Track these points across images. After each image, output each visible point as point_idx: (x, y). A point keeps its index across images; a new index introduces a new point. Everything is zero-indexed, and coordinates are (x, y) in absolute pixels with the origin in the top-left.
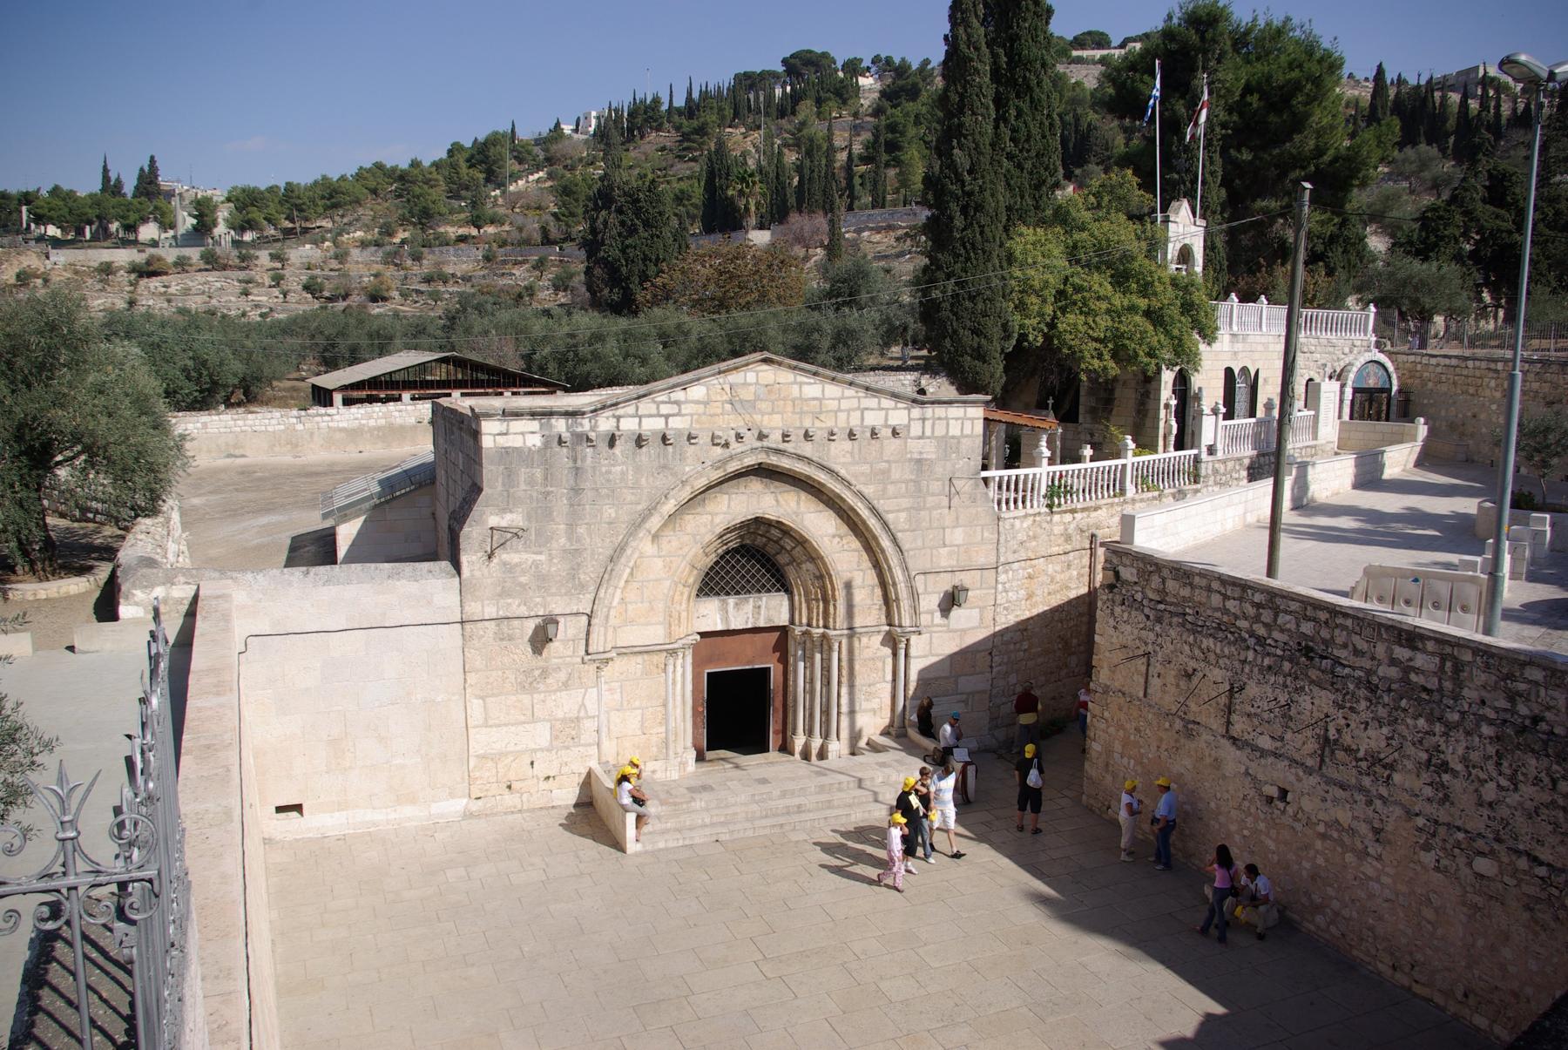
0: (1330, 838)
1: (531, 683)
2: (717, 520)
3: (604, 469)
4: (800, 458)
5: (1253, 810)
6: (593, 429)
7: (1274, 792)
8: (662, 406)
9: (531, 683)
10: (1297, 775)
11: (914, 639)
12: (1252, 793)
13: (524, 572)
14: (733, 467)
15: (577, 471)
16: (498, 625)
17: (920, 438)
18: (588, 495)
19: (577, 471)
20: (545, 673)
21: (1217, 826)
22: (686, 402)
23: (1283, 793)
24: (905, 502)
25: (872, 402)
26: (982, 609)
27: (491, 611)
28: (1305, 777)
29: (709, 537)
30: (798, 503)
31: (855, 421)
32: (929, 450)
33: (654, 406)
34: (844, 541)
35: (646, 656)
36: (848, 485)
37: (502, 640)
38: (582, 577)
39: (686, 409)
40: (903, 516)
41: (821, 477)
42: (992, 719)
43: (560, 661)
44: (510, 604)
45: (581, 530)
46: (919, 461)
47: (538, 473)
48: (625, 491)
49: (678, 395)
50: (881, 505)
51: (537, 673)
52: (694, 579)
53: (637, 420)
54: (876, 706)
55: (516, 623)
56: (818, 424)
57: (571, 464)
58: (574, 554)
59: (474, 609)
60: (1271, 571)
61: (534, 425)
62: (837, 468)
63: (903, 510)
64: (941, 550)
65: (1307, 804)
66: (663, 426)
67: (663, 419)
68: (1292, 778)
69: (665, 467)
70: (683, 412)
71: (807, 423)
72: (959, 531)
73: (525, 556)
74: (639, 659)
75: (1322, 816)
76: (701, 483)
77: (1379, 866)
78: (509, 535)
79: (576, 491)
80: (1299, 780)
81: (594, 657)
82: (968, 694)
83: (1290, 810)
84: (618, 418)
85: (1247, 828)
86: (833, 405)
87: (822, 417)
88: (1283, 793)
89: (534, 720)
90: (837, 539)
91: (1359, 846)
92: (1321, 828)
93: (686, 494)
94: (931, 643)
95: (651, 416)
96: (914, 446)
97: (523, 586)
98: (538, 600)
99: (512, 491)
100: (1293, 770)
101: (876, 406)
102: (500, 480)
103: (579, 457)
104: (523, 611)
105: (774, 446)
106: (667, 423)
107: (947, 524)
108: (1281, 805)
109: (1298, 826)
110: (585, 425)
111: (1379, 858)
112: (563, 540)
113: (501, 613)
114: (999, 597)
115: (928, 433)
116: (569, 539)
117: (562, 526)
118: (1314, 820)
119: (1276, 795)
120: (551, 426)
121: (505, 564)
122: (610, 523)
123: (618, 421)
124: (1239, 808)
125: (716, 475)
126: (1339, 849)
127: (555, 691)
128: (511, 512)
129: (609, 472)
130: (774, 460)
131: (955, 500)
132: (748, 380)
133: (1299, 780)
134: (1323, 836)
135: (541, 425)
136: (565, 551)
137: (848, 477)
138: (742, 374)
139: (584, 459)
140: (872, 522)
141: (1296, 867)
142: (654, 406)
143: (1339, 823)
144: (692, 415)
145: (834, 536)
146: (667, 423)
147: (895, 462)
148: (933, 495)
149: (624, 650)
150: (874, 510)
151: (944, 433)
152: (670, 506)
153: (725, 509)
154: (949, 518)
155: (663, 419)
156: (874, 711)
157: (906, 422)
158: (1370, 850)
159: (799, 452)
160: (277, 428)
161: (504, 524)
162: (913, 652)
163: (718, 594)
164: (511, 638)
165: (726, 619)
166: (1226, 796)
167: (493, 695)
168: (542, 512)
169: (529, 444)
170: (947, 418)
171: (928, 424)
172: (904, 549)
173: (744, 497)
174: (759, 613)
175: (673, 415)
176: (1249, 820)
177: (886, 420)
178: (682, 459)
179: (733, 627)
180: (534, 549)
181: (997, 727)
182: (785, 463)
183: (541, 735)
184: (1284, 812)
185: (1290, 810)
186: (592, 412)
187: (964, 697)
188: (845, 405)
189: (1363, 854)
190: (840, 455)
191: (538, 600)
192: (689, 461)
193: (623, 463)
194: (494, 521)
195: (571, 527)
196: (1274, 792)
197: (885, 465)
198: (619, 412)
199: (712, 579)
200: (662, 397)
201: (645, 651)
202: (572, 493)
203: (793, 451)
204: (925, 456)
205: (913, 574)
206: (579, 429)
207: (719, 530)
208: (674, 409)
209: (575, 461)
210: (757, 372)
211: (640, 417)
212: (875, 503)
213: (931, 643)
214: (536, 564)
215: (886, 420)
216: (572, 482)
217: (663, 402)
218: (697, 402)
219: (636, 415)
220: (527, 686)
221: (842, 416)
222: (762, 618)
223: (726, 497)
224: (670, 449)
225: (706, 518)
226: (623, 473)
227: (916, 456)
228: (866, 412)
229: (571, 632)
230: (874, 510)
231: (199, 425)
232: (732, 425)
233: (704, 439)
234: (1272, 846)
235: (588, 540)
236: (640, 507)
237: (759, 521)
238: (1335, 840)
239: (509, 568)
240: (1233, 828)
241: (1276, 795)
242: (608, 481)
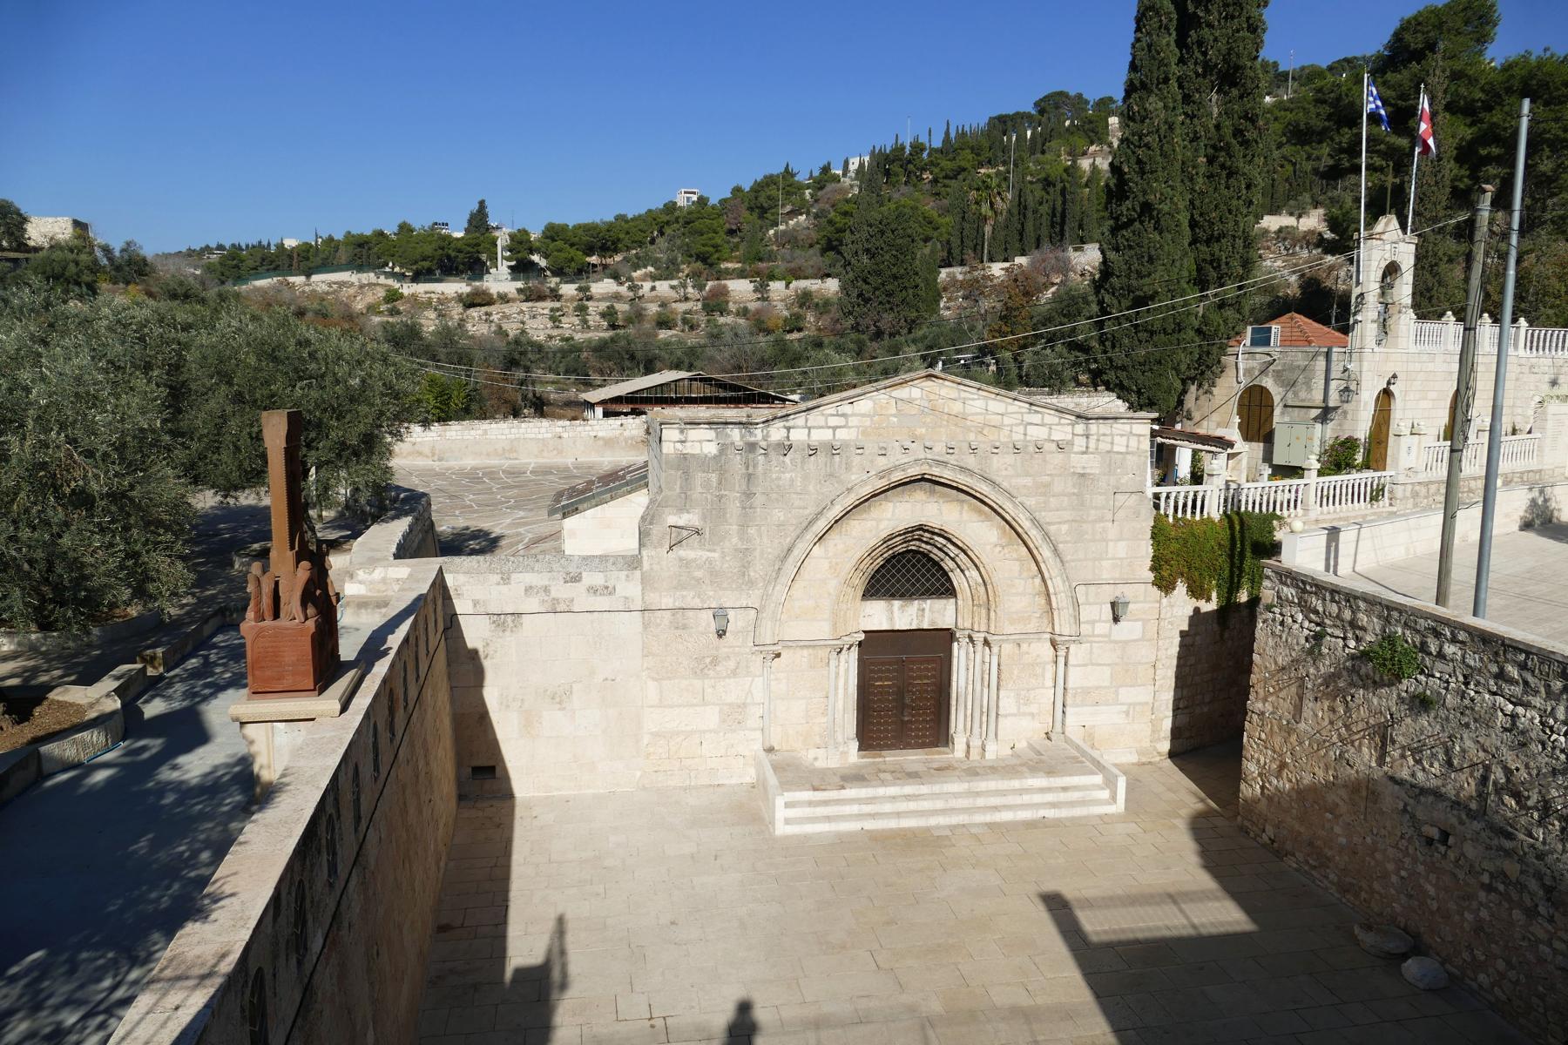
0: (1496, 890)
1: (702, 670)
2: (882, 527)
3: (774, 476)
4: (963, 469)
5: (1411, 851)
6: (765, 438)
7: (1434, 833)
8: (829, 418)
9: (702, 670)
10: (1460, 818)
11: (1073, 648)
12: (1410, 832)
13: (699, 567)
14: (897, 476)
15: (749, 477)
16: (673, 615)
17: (1083, 453)
18: (759, 500)
19: (749, 477)
20: (715, 661)
21: (1373, 863)
22: (853, 415)
23: (1445, 835)
24: (1067, 515)
25: (1036, 418)
26: (1145, 622)
27: (667, 602)
28: (1467, 821)
29: (873, 542)
30: (961, 514)
31: (1017, 437)
32: (1092, 464)
33: (823, 418)
34: (1006, 550)
35: (811, 651)
36: (1011, 496)
37: (677, 628)
38: (752, 574)
39: (853, 421)
40: (1064, 528)
41: (983, 488)
42: (1153, 731)
43: (731, 650)
44: (683, 597)
45: (752, 531)
46: (1083, 475)
47: (714, 477)
48: (794, 496)
49: (846, 408)
50: (1044, 516)
51: (708, 660)
52: (860, 583)
53: (807, 430)
54: (1035, 711)
55: (690, 613)
56: (981, 438)
57: (744, 471)
58: (744, 555)
59: (654, 599)
60: (1441, 598)
61: (711, 434)
62: (998, 480)
63: (1065, 522)
64: (1104, 563)
65: (1470, 850)
66: (831, 437)
68: (1454, 821)
69: (831, 475)
70: (850, 424)
71: (972, 437)
72: (1122, 544)
73: (700, 553)
74: (805, 652)
75: (1486, 865)
76: (867, 490)
77: (1550, 928)
78: (685, 533)
79: (749, 495)
80: (1462, 823)
81: (761, 648)
82: (1130, 704)
83: (1452, 855)
84: (788, 429)
85: (1404, 869)
86: (996, 420)
87: (985, 432)
88: (1445, 835)
89: (704, 702)
90: (999, 549)
91: (1528, 902)
92: (1486, 878)
93: (851, 499)
94: (1091, 652)
96: (1078, 462)
97: (698, 580)
98: (711, 593)
99: (689, 493)
100: (1455, 812)
101: (1039, 422)
102: (678, 483)
103: (751, 463)
104: (697, 603)
105: (937, 458)
106: (834, 434)
107: (1109, 537)
108: (1442, 849)
109: (1461, 875)
110: (758, 434)
111: (1551, 920)
112: (735, 540)
113: (678, 604)
114: (1163, 612)
115: (1092, 445)
116: (740, 539)
117: (735, 527)
118: (1478, 869)
119: (1436, 837)
120: (728, 436)
121: (681, 559)
122: (779, 526)
123: (789, 432)
124: (1396, 846)
126: (1507, 906)
127: (725, 678)
128: (688, 512)
129: (779, 478)
130: (936, 471)
131: (1121, 514)
132: (913, 396)
133: (1462, 823)
134: (1489, 888)
135: (717, 434)
136: (736, 550)
137: (1011, 490)
138: (907, 389)
139: (755, 466)
140: (1033, 533)
141: (1457, 918)
142: (823, 418)
143: (1506, 876)
144: (858, 427)
145: (996, 546)
146: (834, 434)
147: (1060, 475)
148: (1096, 508)
149: (790, 644)
150: (1035, 521)
151: (1108, 447)
152: (836, 511)
153: (889, 516)
154: (1113, 530)
155: (831, 430)
156: (1032, 715)
157: (1069, 437)
158: (1541, 909)
159: (962, 464)
160: (545, 435)
161: (681, 523)
162: (1071, 660)
164: (685, 627)
165: (891, 619)
166: (1383, 832)
167: (670, 679)
168: (717, 511)
169: (706, 451)
170: (1112, 435)
171: (1092, 440)
172: (1065, 560)
173: (908, 506)
174: (923, 616)
175: (840, 427)
176: (1407, 860)
177: (1050, 434)
178: (848, 468)
179: (897, 627)
180: (707, 547)
181: (1159, 740)
182: (947, 474)
183: (711, 717)
184: (1445, 856)
185: (1452, 855)
186: (764, 422)
187: (1125, 708)
188: (1007, 421)
189: (1531, 913)
190: (1003, 467)
191: (711, 593)
192: (854, 470)
193: (792, 471)
194: (672, 520)
195: (743, 527)
196: (1434, 833)
197: (1047, 479)
198: (787, 424)
199: (878, 581)
200: (830, 410)
201: (811, 645)
202: (743, 498)
203: (955, 463)
204: (1088, 471)
205: (1074, 584)
206: (752, 439)
207: (884, 535)
209: (747, 468)
211: (809, 428)
212: (1037, 515)
213: (1091, 652)
214: (709, 561)
215: (1050, 434)
216: (744, 487)
217: (834, 415)
218: (863, 415)
219: (806, 427)
220: (698, 672)
221: (1006, 431)
222: (926, 619)
223: (891, 505)
224: (837, 457)
225: (870, 524)
226: (792, 480)
227: (1080, 471)
228: (1028, 427)
229: (740, 624)
230: (1035, 521)
231: (480, 432)
233: (871, 448)
234: (1431, 890)
235: (758, 540)
236: (807, 512)
238: (1501, 894)
239: (685, 563)
240: (1390, 867)
241: (1436, 837)
242: (778, 486)
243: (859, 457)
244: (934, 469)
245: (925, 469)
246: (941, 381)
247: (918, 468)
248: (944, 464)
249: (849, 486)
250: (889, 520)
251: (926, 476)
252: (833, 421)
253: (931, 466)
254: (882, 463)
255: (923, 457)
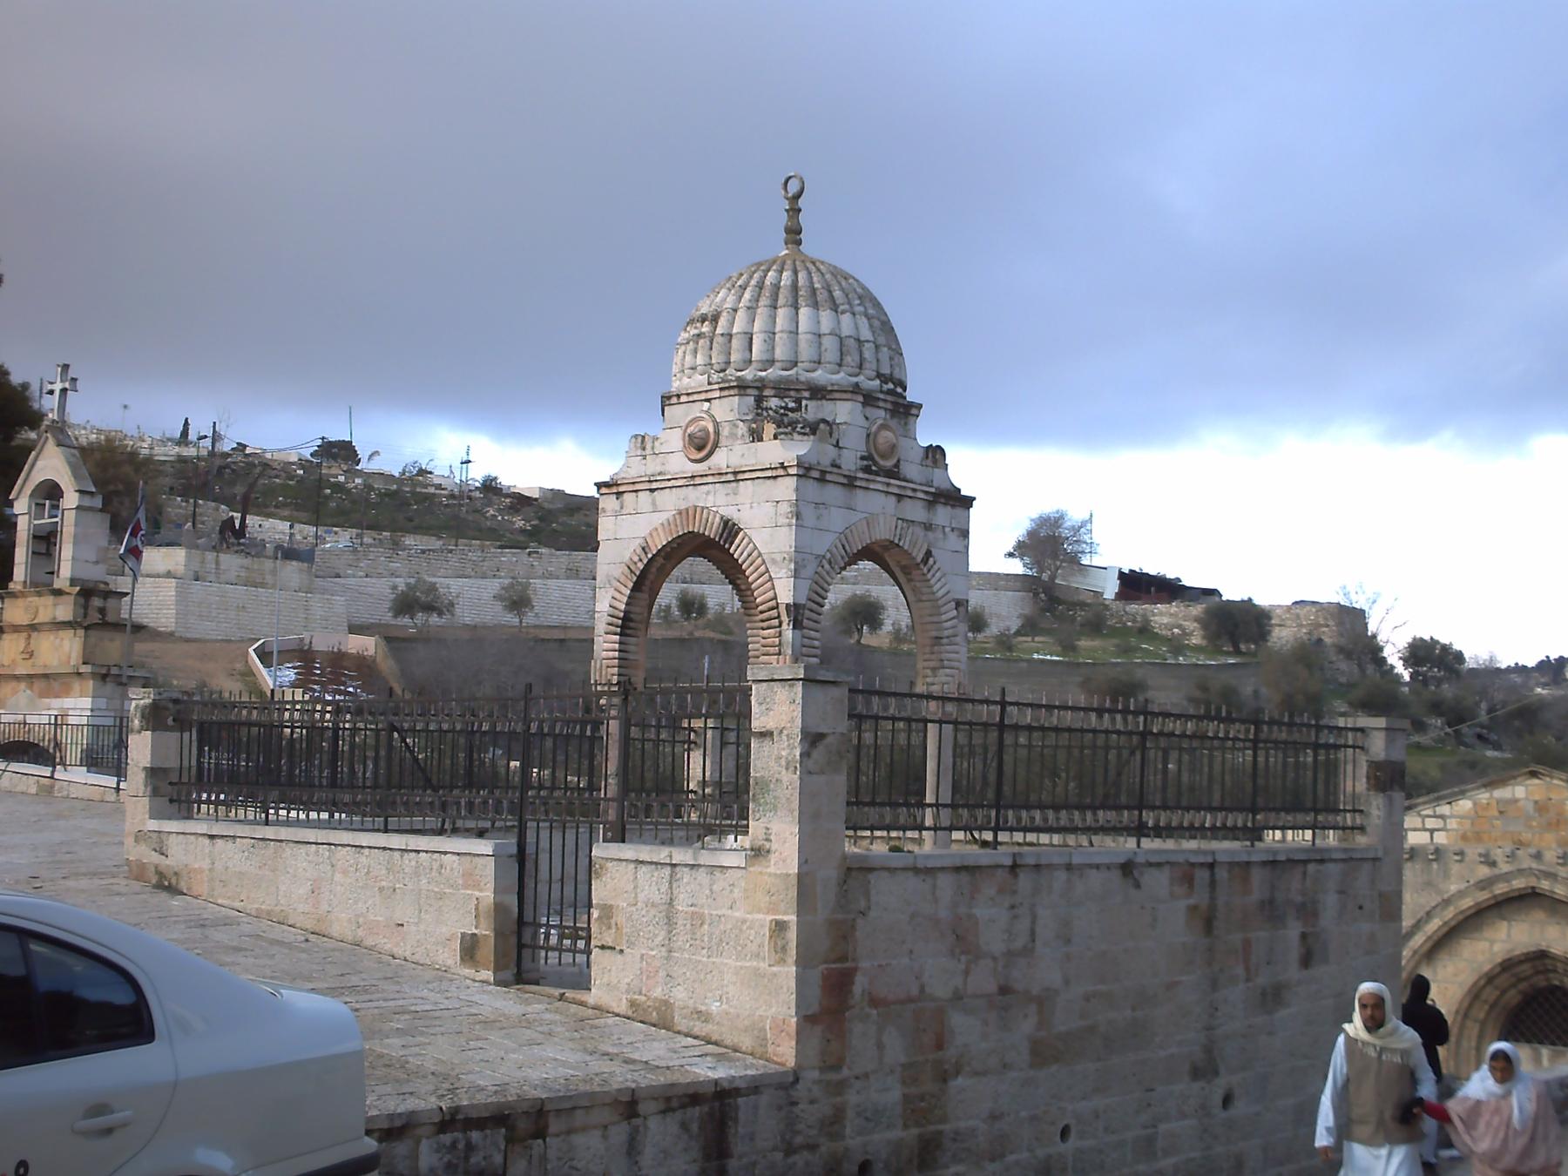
2: (1497, 947)
8: (1427, 820)
14: (1500, 889)
22: (1451, 816)
33: (1420, 820)
39: (1452, 824)
49: (1445, 809)
66: (1429, 841)
67: (1428, 834)
69: (1429, 884)
76: (1467, 903)
93: (1449, 913)
95: (1415, 830)
125: (1483, 896)
130: (1545, 885)
155: (1428, 834)
163: (1529, 1041)
178: (1446, 875)
192: (1453, 879)
208: (1438, 823)
210: (1526, 786)
223: (1505, 923)
224: (1435, 865)
225: (1483, 945)
232: (1500, 843)
237: (1542, 955)
243: (1457, 865)
244: (1543, 882)
245: (1533, 882)
246: (1548, 779)
247: (1523, 880)
248: (1552, 876)
249: (1446, 896)
250: (1503, 941)
251: (1537, 891)
252: (1430, 823)
253: (1538, 878)
254: (1484, 871)
255: (1525, 866)
